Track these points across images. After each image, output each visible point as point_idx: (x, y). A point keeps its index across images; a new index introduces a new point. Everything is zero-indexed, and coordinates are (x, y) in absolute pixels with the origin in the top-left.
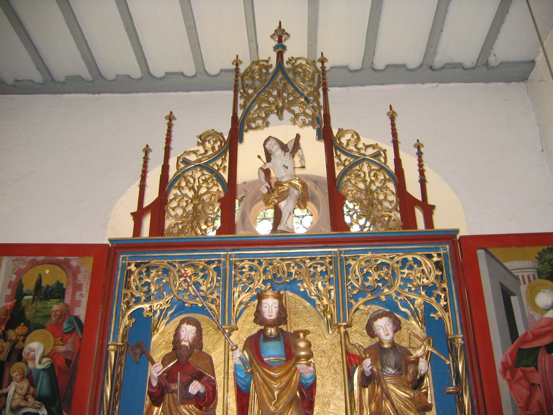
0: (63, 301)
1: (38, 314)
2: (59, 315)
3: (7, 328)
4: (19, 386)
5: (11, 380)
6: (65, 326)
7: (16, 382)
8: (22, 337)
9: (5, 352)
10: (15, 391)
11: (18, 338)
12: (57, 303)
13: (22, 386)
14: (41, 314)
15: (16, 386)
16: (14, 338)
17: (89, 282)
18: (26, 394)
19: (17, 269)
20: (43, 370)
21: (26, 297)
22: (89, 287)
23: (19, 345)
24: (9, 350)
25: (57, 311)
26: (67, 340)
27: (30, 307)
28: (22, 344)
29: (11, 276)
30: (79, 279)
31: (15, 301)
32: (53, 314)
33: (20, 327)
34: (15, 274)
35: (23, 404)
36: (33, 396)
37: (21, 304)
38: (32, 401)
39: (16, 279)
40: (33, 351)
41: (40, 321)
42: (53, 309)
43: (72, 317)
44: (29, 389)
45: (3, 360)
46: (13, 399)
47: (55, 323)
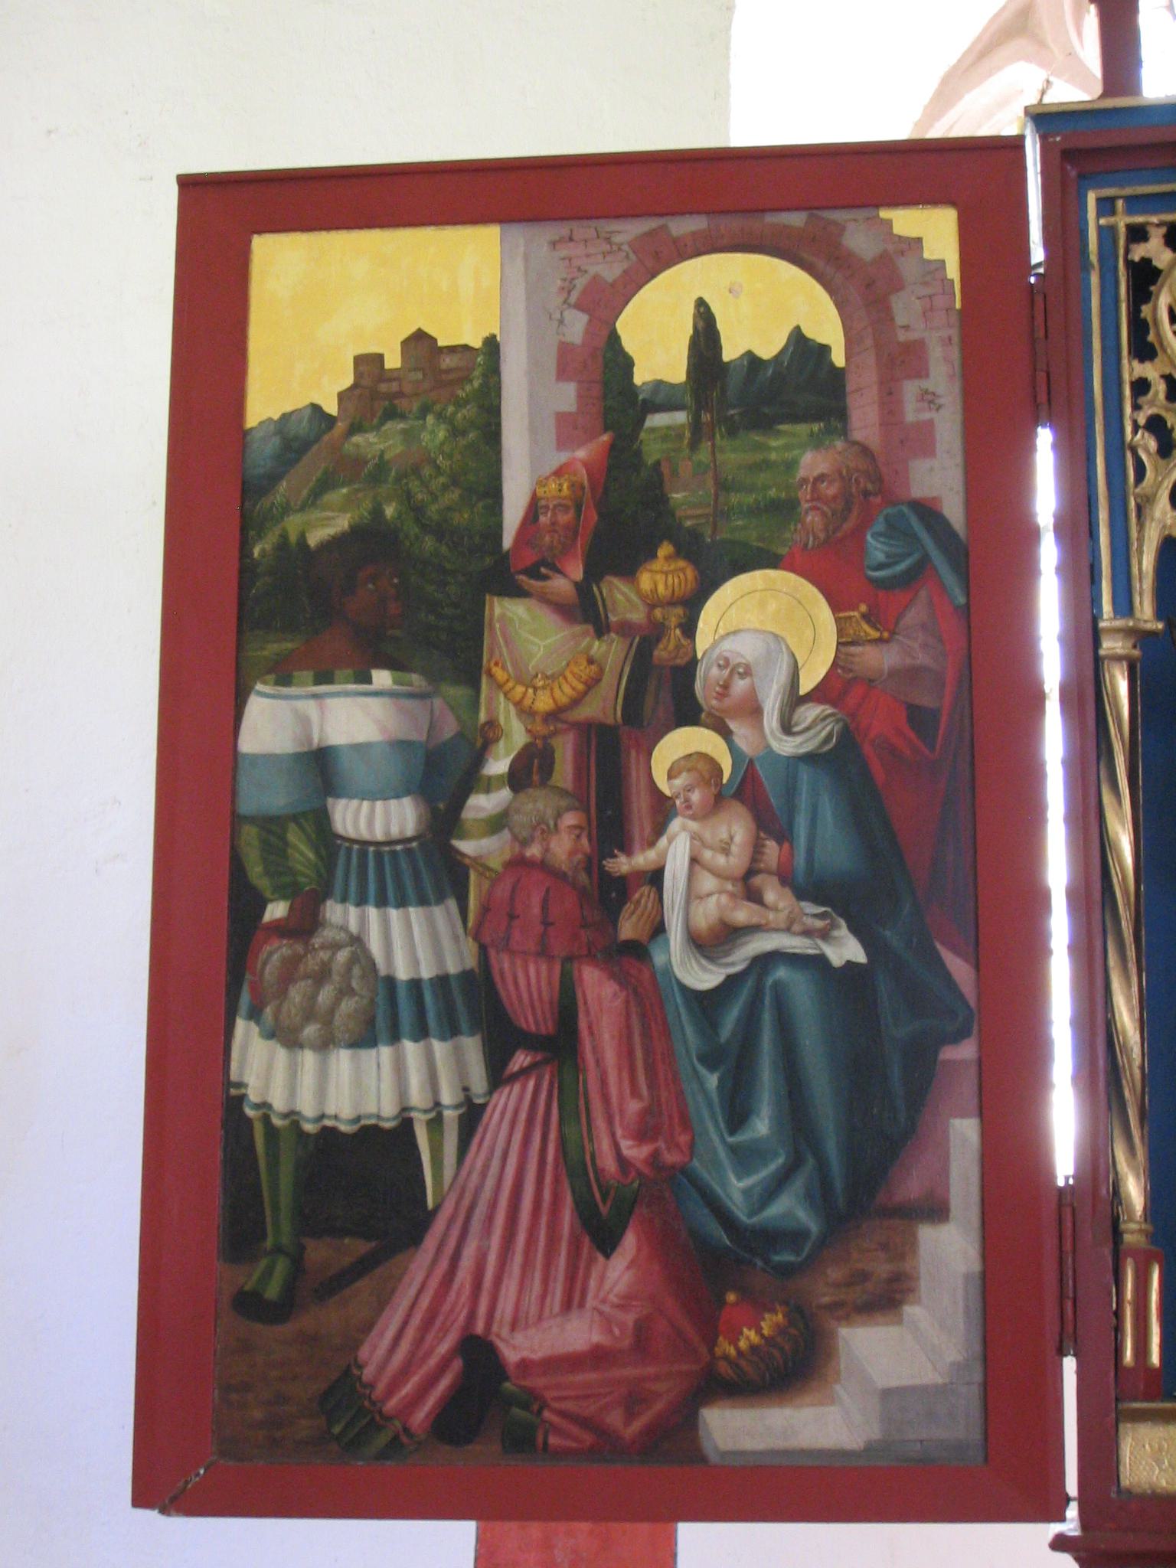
0: (844, 432)
1: (734, 499)
2: (835, 498)
3: (595, 572)
4: (707, 835)
5: (663, 809)
6: (877, 549)
7: (693, 818)
8: (679, 611)
9: (608, 679)
10: (694, 861)
11: (658, 613)
12: (816, 442)
13: (725, 836)
14: (750, 499)
15: (692, 838)
16: (637, 616)
17: (954, 333)
18: (750, 873)
19: (581, 283)
20: (810, 758)
21: (657, 420)
22: (955, 353)
23: (671, 646)
24: (627, 669)
25: (821, 478)
26: (897, 623)
27: (685, 469)
28: (684, 642)
29: (561, 322)
30: (901, 319)
31: (605, 438)
32: (805, 494)
33: (658, 564)
34: (579, 306)
35: (742, 915)
36: (785, 878)
37: (638, 453)
38: (781, 905)
39: (589, 332)
40: (742, 676)
41: (745, 530)
42: (801, 473)
43: (905, 509)
44: (757, 849)
45: (610, 721)
46: (692, 895)
47: (822, 536)
